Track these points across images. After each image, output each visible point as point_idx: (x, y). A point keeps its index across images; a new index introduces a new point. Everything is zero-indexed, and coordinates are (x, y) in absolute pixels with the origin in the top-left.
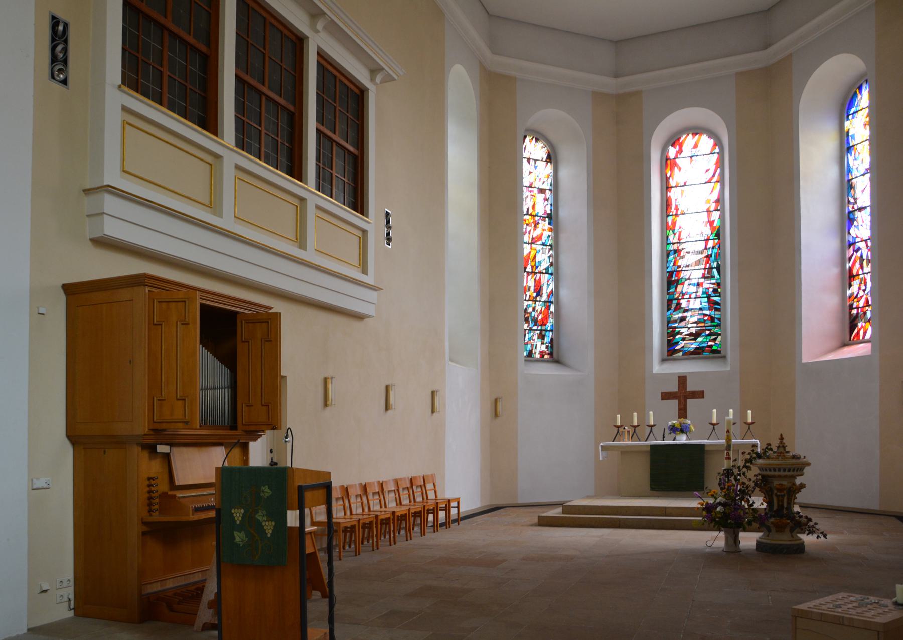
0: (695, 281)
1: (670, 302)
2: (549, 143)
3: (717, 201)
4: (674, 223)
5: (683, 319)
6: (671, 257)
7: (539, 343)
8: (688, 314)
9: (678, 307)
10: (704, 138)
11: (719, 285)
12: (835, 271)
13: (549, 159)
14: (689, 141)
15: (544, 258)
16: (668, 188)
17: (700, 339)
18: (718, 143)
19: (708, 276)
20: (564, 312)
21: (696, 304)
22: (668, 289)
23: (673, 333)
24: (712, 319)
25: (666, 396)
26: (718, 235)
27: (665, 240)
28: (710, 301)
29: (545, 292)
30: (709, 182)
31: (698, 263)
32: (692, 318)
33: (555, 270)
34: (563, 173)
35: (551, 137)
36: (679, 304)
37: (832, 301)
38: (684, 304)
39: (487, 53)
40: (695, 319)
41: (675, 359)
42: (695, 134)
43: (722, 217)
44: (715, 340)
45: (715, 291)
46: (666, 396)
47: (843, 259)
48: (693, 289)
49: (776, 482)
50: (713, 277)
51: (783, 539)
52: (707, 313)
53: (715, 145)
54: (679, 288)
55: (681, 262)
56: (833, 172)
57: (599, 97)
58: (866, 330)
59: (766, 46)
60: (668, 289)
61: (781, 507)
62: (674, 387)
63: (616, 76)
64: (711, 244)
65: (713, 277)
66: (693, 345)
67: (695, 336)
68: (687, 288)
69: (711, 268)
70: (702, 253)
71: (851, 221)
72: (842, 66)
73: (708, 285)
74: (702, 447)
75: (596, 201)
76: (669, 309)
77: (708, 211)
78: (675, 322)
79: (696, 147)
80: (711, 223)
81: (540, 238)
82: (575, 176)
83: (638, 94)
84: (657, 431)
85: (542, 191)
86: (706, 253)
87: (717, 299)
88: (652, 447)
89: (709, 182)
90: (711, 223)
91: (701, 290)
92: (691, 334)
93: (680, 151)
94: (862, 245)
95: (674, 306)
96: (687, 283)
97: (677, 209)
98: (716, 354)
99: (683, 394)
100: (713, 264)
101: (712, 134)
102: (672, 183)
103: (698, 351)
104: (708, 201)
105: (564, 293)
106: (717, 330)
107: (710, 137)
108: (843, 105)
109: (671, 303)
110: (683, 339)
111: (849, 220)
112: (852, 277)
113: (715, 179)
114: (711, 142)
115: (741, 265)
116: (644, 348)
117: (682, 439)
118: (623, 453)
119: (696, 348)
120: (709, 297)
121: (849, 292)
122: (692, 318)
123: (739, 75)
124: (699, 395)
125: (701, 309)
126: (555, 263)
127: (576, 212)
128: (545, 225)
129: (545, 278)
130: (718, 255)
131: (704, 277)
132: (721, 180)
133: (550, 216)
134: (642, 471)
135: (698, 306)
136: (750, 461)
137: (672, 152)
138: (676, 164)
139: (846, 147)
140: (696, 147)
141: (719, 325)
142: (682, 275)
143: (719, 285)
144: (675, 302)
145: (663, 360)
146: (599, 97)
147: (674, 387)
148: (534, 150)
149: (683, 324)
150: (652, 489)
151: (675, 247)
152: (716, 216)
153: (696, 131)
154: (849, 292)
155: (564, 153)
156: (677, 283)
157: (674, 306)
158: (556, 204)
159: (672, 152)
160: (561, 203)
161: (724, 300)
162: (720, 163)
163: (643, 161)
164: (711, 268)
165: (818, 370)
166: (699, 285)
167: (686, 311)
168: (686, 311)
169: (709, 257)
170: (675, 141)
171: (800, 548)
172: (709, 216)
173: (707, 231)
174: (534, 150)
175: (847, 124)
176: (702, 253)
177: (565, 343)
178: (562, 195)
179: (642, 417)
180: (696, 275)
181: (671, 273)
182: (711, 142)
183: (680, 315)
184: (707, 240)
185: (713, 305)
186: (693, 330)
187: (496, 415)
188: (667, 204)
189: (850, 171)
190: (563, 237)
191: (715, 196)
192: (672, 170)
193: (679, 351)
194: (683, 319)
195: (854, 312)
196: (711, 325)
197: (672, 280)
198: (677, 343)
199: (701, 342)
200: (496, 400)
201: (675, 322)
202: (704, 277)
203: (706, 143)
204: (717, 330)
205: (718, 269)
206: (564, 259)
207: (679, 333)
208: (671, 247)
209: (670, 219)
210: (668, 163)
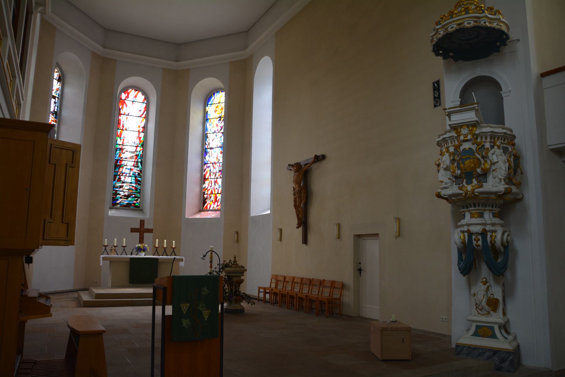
0: (129, 167)
1: (115, 176)
2: (61, 70)
3: (144, 127)
4: (121, 134)
5: (121, 187)
6: (118, 152)
8: (125, 185)
9: (119, 180)
10: (140, 94)
11: (141, 171)
12: (199, 175)
14: (133, 93)
17: (129, 199)
18: (147, 98)
19: (136, 166)
21: (128, 180)
22: (115, 169)
23: (116, 194)
24: (136, 189)
25: (133, 230)
26: (142, 145)
28: (136, 180)
30: (140, 117)
31: (131, 158)
32: (126, 187)
34: (67, 91)
35: (64, 68)
36: (120, 179)
38: (122, 178)
40: (128, 188)
41: (116, 209)
42: (136, 90)
44: (137, 200)
45: (139, 174)
46: (133, 230)
48: (128, 171)
49: (235, 279)
50: (138, 167)
51: (235, 306)
52: (134, 185)
53: (145, 99)
54: (121, 169)
55: (122, 156)
56: (200, 128)
57: (95, 55)
59: (177, 61)
60: (115, 169)
61: (236, 291)
62: (138, 226)
63: (104, 47)
64: (139, 149)
65: (138, 167)
67: (127, 197)
68: (124, 170)
69: (137, 162)
70: (133, 152)
72: (210, 82)
73: (135, 170)
74: (157, 259)
75: (87, 112)
76: (114, 180)
77: (139, 132)
78: (117, 187)
79: (136, 97)
80: (140, 138)
84: (128, 250)
85: (54, 97)
86: (136, 153)
87: (139, 178)
88: (131, 259)
89: (140, 117)
90: (140, 138)
91: (132, 173)
92: (125, 196)
93: (128, 97)
94: (211, 165)
95: (117, 179)
96: (125, 167)
97: (123, 127)
98: (138, 208)
99: (141, 230)
100: (140, 160)
101: (144, 93)
102: (122, 112)
103: (128, 205)
104: (139, 127)
106: (138, 195)
107: (143, 95)
108: (206, 99)
109: (117, 177)
110: (121, 198)
111: (204, 152)
113: (144, 116)
115: (157, 164)
117: (142, 255)
118: (111, 262)
119: (127, 204)
120: (135, 177)
121: (204, 186)
122: (126, 187)
123: (164, 69)
124: (150, 231)
125: (131, 183)
130: (142, 156)
131: (134, 166)
132: (147, 118)
133: (55, 113)
134: (124, 273)
135: (130, 181)
136: (223, 268)
137: (123, 96)
138: (124, 103)
139: (206, 119)
140: (136, 97)
141: (139, 193)
142: (123, 162)
143: (141, 171)
144: (118, 177)
146: (95, 55)
147: (138, 226)
149: (121, 189)
150: (130, 283)
151: (120, 147)
152: (142, 135)
153: (137, 89)
154: (204, 186)
155: (69, 78)
156: (120, 166)
157: (117, 179)
158: (60, 107)
159: (123, 96)
160: (63, 108)
161: (144, 179)
162: (147, 109)
164: (137, 162)
166: (131, 170)
167: (123, 182)
168: (123, 182)
169: (137, 155)
170: (125, 90)
171: (241, 311)
172: (139, 135)
173: (137, 141)
175: (207, 108)
176: (133, 152)
178: (65, 103)
179: (120, 241)
180: (130, 164)
181: (117, 161)
182: (143, 97)
183: (120, 184)
184: (137, 147)
185: (137, 181)
186: (126, 194)
189: (207, 130)
191: (142, 125)
192: (122, 105)
193: (118, 204)
194: (121, 187)
195: (206, 196)
196: (137, 192)
197: (118, 165)
198: (117, 200)
199: (130, 201)
201: (117, 187)
202: (134, 166)
203: (141, 97)
204: (138, 195)
205: (141, 163)
207: (119, 194)
209: (119, 131)
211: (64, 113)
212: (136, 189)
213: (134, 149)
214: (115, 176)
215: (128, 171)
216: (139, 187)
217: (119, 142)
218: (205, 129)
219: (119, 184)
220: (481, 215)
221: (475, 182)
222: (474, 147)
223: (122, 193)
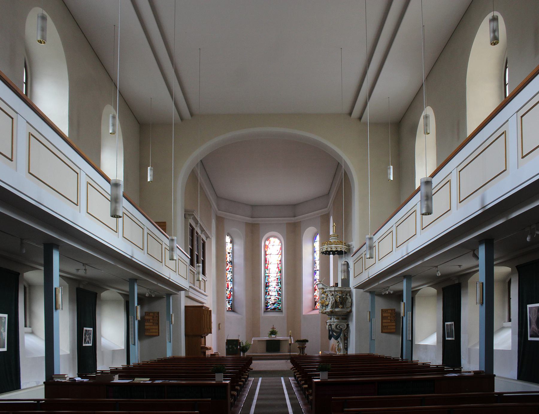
2: (231, 237)
5: (270, 298)
7: (228, 304)
13: (231, 242)
15: (229, 276)
16: (266, 255)
18: (281, 242)
20: (236, 294)
23: (267, 303)
24: (279, 299)
27: (265, 272)
29: (230, 287)
31: (274, 280)
32: (273, 298)
33: (233, 280)
34: (235, 247)
37: (310, 296)
38: (270, 293)
39: (217, 210)
43: (281, 266)
47: (313, 284)
48: (273, 289)
58: (318, 305)
66: (273, 307)
67: (274, 304)
71: (315, 273)
73: (277, 288)
75: (246, 259)
80: (278, 268)
81: (228, 269)
82: (239, 248)
83: (258, 224)
85: (229, 253)
90: (278, 268)
91: (275, 289)
98: (280, 310)
100: (279, 282)
102: (267, 253)
103: (275, 309)
105: (235, 288)
112: (315, 290)
114: (279, 241)
115: (287, 284)
116: (259, 308)
122: (273, 298)
126: (233, 278)
127: (239, 261)
128: (229, 265)
129: (230, 283)
133: (231, 262)
142: (270, 284)
145: (264, 312)
148: (228, 239)
152: (280, 265)
155: (236, 240)
158: (233, 258)
159: (267, 243)
162: (281, 249)
163: (259, 246)
165: (307, 317)
173: (277, 270)
174: (228, 239)
177: (236, 305)
178: (235, 255)
185: (279, 294)
187: (219, 329)
188: (266, 260)
190: (235, 269)
194: (270, 298)
196: (278, 302)
197: (267, 286)
200: (219, 324)
206: (235, 276)
208: (266, 275)
210: (266, 247)
211: (236, 261)
212: (279, 299)
213: (275, 275)
214: (266, 292)
215: (273, 289)
216: (280, 298)
217: (267, 272)
218: (314, 258)
219: (268, 297)
220: (331, 319)
221: (324, 308)
222: (325, 296)
223: (271, 302)
